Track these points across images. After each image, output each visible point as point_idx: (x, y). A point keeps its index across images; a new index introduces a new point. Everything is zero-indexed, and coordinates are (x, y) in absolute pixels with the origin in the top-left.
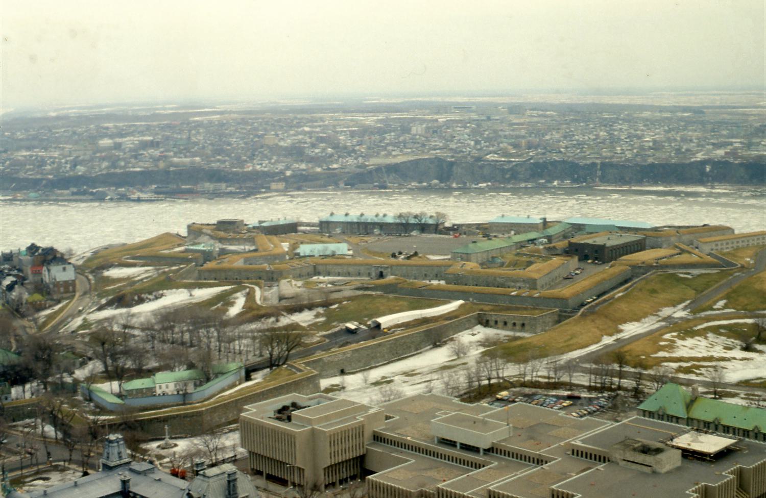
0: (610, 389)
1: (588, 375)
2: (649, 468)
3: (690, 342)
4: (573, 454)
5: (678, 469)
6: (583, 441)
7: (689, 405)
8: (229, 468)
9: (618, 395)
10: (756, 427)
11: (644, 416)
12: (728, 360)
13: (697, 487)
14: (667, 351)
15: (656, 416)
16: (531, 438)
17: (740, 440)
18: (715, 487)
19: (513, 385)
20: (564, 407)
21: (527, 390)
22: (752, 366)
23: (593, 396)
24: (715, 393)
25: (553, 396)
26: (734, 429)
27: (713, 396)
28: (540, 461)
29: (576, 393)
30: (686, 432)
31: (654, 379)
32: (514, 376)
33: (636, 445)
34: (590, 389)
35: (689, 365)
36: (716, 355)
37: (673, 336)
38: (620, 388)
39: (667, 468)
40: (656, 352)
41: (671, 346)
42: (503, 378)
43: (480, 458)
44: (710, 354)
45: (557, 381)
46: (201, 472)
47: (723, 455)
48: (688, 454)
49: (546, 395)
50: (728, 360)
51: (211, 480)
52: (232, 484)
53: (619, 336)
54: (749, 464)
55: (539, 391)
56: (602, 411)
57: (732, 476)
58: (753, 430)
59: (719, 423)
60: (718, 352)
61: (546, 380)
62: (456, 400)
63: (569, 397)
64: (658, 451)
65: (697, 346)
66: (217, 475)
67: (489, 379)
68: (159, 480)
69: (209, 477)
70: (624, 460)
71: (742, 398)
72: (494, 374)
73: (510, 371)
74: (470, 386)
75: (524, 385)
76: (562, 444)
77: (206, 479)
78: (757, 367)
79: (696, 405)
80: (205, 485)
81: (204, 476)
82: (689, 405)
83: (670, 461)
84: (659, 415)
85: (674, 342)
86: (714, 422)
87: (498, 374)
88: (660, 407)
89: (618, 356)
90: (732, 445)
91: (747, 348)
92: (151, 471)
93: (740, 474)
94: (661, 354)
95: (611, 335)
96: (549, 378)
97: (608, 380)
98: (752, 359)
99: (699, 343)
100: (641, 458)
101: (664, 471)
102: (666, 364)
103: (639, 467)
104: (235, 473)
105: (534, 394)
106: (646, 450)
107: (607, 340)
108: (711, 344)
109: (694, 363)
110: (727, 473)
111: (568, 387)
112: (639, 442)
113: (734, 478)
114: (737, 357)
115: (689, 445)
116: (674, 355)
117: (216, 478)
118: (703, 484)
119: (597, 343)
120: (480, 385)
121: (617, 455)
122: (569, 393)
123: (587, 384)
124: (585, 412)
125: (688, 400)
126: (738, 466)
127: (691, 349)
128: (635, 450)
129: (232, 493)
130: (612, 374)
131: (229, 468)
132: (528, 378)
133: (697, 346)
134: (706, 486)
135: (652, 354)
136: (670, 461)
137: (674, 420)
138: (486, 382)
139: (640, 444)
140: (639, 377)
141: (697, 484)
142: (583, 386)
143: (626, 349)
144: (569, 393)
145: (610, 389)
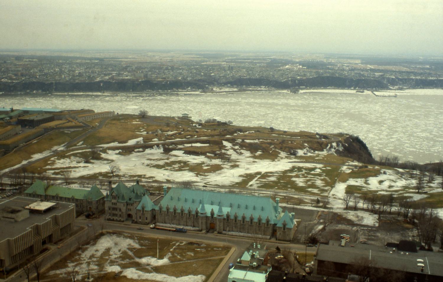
1: (10, 179)
2: (13, 220)
3: (62, 161)
5: (28, 218)
7: (46, 189)
10: (73, 196)
11: (27, 196)
12: (77, 167)
14: (50, 165)
17: (58, 204)
22: (87, 170)
23: (11, 188)
24: (66, 183)
26: (66, 198)
27: (66, 184)
29: (4, 188)
30: (36, 201)
31: (39, 178)
33: (9, 210)
34: (11, 185)
35: (59, 171)
36: (72, 166)
37: (55, 159)
38: (25, 184)
39: (22, 218)
40: (45, 166)
41: (53, 163)
44: (70, 165)
47: (48, 210)
48: (33, 212)
50: (77, 167)
53: (30, 160)
54: (59, 213)
56: (14, 195)
57: (49, 219)
58: (72, 198)
59: (58, 196)
60: (74, 164)
64: (19, 211)
65: (64, 162)
70: (3, 217)
71: (78, 184)
78: (89, 170)
79: (49, 188)
82: (46, 189)
83: (25, 214)
84: (33, 195)
85: (55, 161)
88: (34, 192)
89: (24, 169)
90: (55, 205)
91: (87, 162)
93: (55, 219)
94: (48, 167)
95: (26, 160)
97: (19, 180)
98: (88, 167)
99: (66, 161)
100: (10, 215)
101: (20, 220)
102: (47, 171)
103: (9, 220)
106: (14, 212)
107: (24, 162)
108: (71, 161)
109: (62, 170)
110: (48, 218)
113: (50, 220)
114: (82, 166)
115: (34, 207)
116: (53, 167)
118: (36, 224)
119: (19, 164)
123: (10, 183)
124: (5, 196)
125: (46, 187)
126: (54, 214)
127: (62, 164)
130: (20, 177)
133: (64, 162)
134: (37, 225)
135: (44, 167)
136: (24, 215)
137: (40, 196)
139: (12, 209)
140: (33, 178)
141: (33, 224)
142: (8, 184)
143: (33, 165)
145: (20, 184)
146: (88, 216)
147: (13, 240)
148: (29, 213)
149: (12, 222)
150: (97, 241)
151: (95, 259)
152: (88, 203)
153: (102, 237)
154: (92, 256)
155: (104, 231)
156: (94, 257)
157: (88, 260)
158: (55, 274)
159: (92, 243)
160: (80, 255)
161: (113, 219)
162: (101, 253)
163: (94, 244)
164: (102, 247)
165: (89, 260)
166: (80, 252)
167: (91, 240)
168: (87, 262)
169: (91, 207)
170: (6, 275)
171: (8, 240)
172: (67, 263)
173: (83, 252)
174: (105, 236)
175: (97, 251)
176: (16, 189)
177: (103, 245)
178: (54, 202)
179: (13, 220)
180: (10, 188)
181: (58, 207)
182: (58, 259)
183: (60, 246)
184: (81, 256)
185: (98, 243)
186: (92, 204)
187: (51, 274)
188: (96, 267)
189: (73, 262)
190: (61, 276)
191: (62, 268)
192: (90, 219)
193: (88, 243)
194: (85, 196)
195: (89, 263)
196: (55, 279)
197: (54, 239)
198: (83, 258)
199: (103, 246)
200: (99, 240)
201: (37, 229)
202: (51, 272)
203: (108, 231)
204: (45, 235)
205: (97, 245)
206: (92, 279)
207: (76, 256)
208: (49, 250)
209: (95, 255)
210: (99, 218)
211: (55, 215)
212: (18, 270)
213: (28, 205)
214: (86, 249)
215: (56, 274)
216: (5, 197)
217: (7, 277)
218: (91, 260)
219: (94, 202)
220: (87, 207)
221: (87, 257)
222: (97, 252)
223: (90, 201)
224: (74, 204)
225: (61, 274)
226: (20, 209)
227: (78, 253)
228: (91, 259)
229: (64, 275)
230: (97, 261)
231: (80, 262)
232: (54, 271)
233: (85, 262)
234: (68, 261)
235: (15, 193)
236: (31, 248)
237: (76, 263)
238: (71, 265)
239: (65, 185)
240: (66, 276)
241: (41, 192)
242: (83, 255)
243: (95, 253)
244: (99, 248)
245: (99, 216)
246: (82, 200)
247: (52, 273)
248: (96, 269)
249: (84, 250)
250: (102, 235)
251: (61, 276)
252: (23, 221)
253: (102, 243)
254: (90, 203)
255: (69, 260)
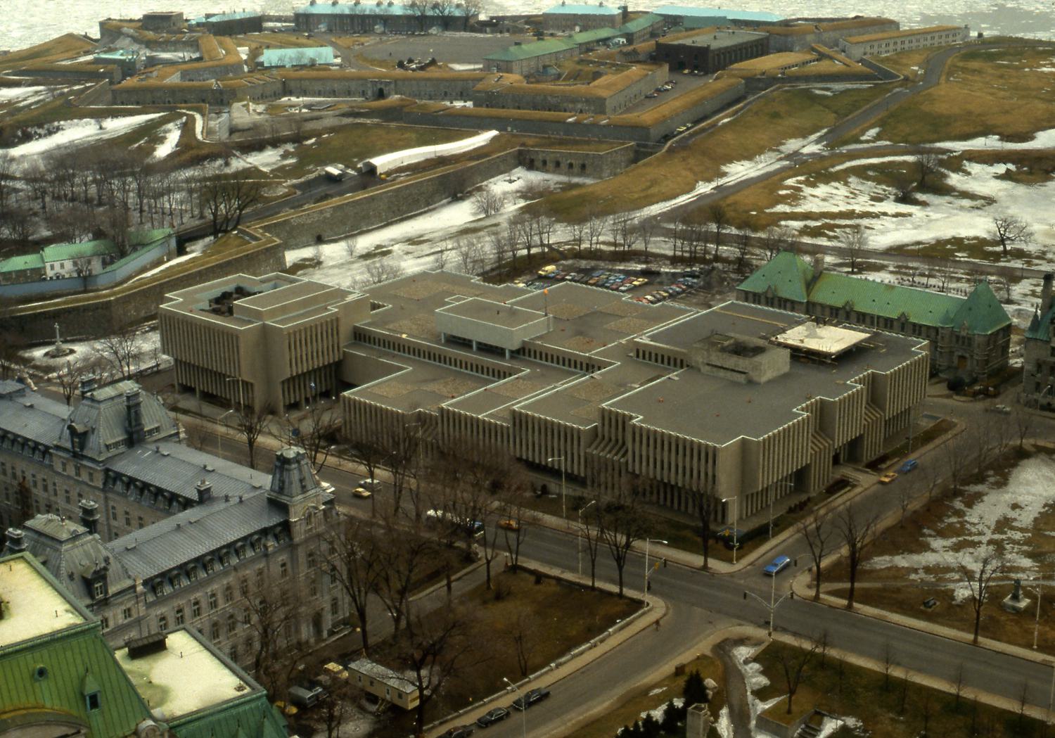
0: (703, 261)
2: (743, 376)
3: (822, 190)
4: (638, 356)
5: (785, 376)
6: (653, 338)
8: (129, 386)
9: (713, 268)
11: (746, 300)
13: (808, 402)
14: (790, 205)
15: (763, 300)
16: (580, 333)
18: (835, 402)
19: (564, 256)
20: (635, 286)
21: (583, 264)
22: (909, 226)
23: (679, 271)
24: (853, 265)
25: (620, 271)
26: (872, 317)
28: (590, 366)
29: (654, 267)
31: (766, 245)
32: (566, 243)
33: (726, 343)
34: (674, 260)
35: (818, 224)
36: (858, 209)
37: (799, 182)
38: (717, 258)
39: (768, 375)
40: (773, 206)
41: (795, 197)
42: (549, 246)
43: (505, 364)
44: (850, 207)
45: (626, 249)
46: (89, 394)
47: (849, 356)
48: (801, 356)
49: (610, 270)
51: (102, 406)
52: (133, 411)
53: (721, 181)
55: (602, 264)
56: (690, 293)
57: (859, 387)
58: (899, 319)
59: (852, 310)
61: (612, 248)
62: (476, 280)
63: (644, 273)
64: (758, 350)
66: (112, 398)
67: (529, 248)
68: (31, 406)
69: (99, 402)
70: (708, 364)
71: (891, 272)
72: (536, 238)
73: (560, 235)
74: (500, 259)
75: (579, 255)
76: (623, 341)
77: (96, 405)
79: (819, 285)
80: (94, 413)
81: (92, 399)
83: (773, 365)
84: (767, 298)
85: (800, 189)
86: (844, 308)
87: (541, 241)
89: (714, 210)
90: (865, 340)
91: (905, 199)
92: (21, 393)
93: (873, 384)
95: (709, 180)
96: (615, 244)
98: (910, 215)
99: (835, 191)
101: (764, 379)
102: (783, 223)
103: (729, 374)
104: (137, 395)
105: (593, 269)
106: (741, 350)
107: (704, 188)
108: (852, 193)
109: (828, 221)
110: (854, 382)
111: (643, 258)
112: (730, 338)
115: (802, 341)
117: (109, 403)
119: (688, 192)
120: (514, 255)
121: (699, 359)
122: (644, 266)
123: (670, 253)
124: (665, 294)
125: (809, 277)
127: (824, 200)
128: (723, 350)
129: (133, 423)
130: (707, 237)
131: (129, 386)
132: (585, 245)
133: (831, 196)
136: (773, 365)
137: (788, 305)
138: (525, 252)
139: (732, 341)
140: (744, 242)
141: (809, 399)
142: (665, 257)
143: (731, 200)
144: (644, 266)
145: (703, 261)
146: (956, 387)
147: (759, 442)
148: (788, 360)
149: (736, 384)
150: (1009, 473)
151: (1018, 536)
152: (957, 341)
153: (1026, 461)
154: (1004, 524)
155: (1028, 443)
156: (1012, 528)
157: (993, 533)
158: (891, 567)
159: (992, 480)
160: (960, 514)
161: (1049, 404)
162: (1032, 517)
163: (1002, 483)
164: (1030, 498)
165: (997, 537)
166: (958, 504)
167: (987, 468)
168: (990, 542)
169: (967, 355)
170: (740, 548)
171: (744, 441)
172: (924, 535)
173: (970, 505)
174: (1032, 461)
175: (1015, 506)
176: (693, 275)
177: (1033, 490)
178: (863, 331)
179: (741, 378)
180: (673, 271)
181: (876, 347)
182: (889, 519)
183: (886, 476)
184: (967, 518)
185: (1011, 480)
186: (970, 345)
187: (878, 567)
188: (1027, 563)
189: (942, 534)
190: (913, 576)
191: (911, 552)
192: (965, 395)
193: (980, 479)
194: (946, 319)
195: (999, 547)
196: (899, 584)
197: (868, 454)
198: (974, 524)
199: (1033, 495)
200: (1015, 472)
201: (822, 414)
202: (876, 559)
203: (1041, 443)
204: (842, 436)
205: (1012, 487)
206: (1028, 601)
207: (949, 517)
208: (854, 486)
209: (1015, 520)
210: (995, 396)
211: (873, 373)
212: (766, 539)
213: (784, 331)
214: (978, 497)
215: (897, 569)
216: (664, 298)
217: (738, 559)
218: (1004, 537)
219: (978, 340)
220: (951, 353)
221: (989, 523)
222: (1017, 510)
223: (963, 333)
224: (926, 342)
225: (916, 571)
226: (761, 343)
227: (952, 508)
228: (1005, 533)
229: (922, 575)
230: (1027, 542)
231: (970, 538)
232: (887, 558)
233: (984, 539)
234: (925, 531)
235: (691, 287)
236: (800, 477)
237: (954, 540)
238: (937, 543)
239: (848, 272)
240: (931, 578)
241: (795, 291)
242: (973, 516)
243: (1012, 514)
244: (1021, 499)
245: (995, 387)
246: (936, 329)
247: (881, 562)
248: (1029, 569)
249: (972, 500)
250: (1021, 455)
251: (913, 576)
252: (769, 382)
253: (1028, 483)
254: (967, 341)
255: (928, 528)
